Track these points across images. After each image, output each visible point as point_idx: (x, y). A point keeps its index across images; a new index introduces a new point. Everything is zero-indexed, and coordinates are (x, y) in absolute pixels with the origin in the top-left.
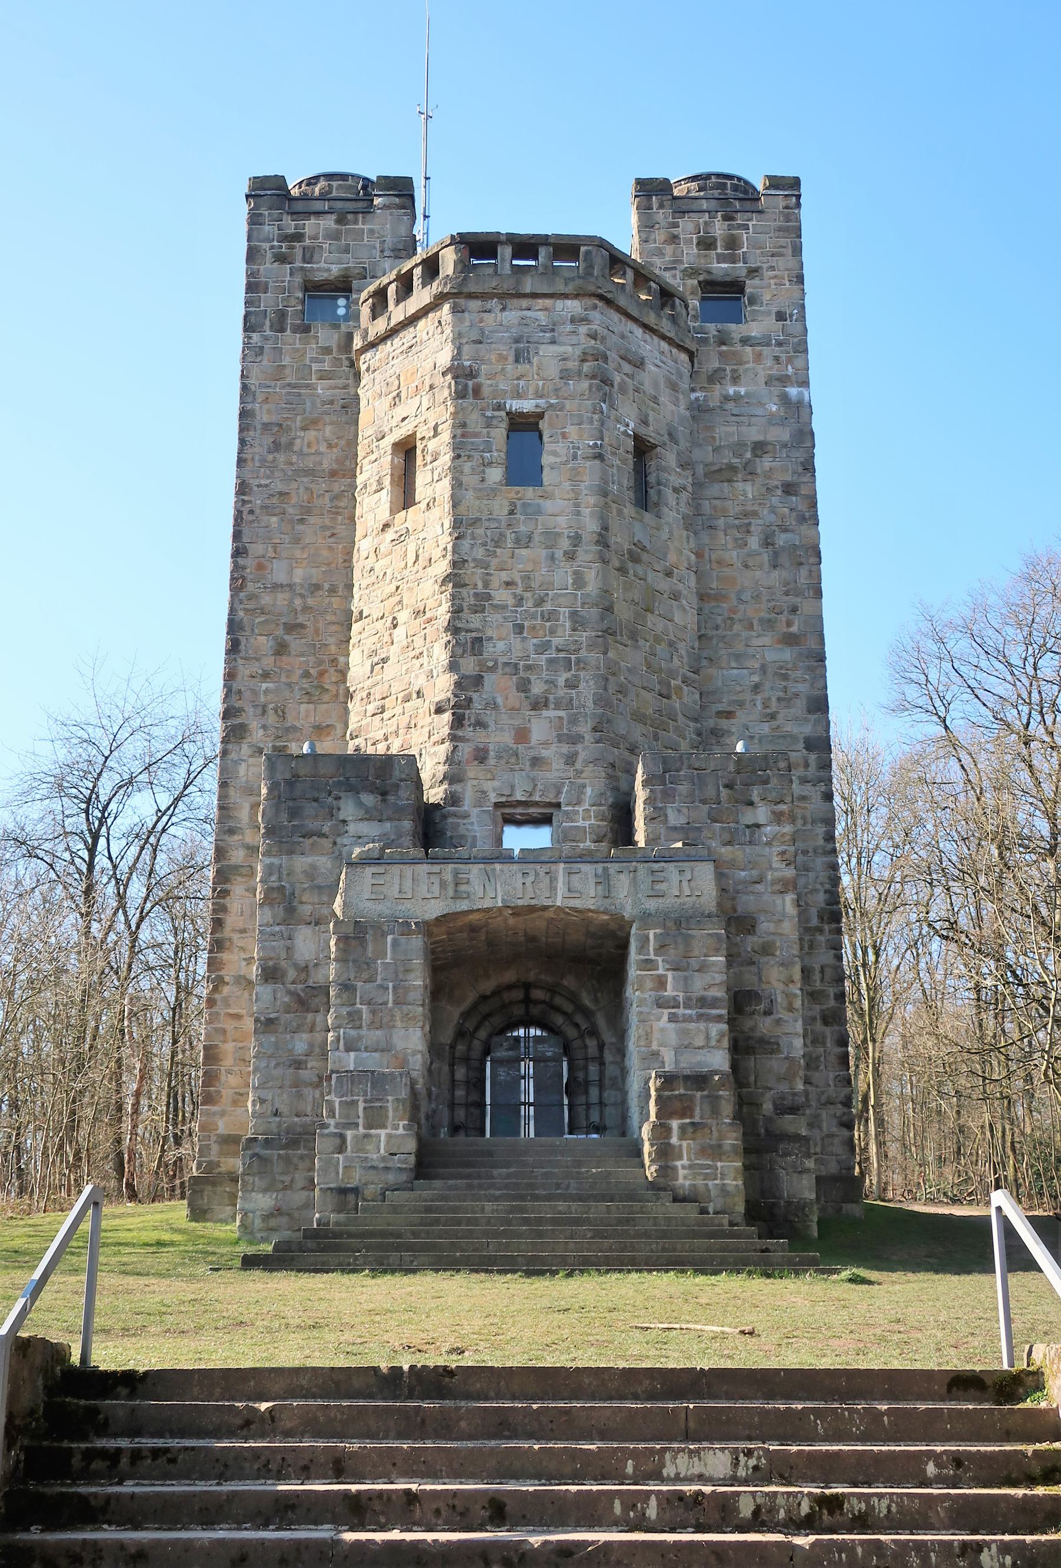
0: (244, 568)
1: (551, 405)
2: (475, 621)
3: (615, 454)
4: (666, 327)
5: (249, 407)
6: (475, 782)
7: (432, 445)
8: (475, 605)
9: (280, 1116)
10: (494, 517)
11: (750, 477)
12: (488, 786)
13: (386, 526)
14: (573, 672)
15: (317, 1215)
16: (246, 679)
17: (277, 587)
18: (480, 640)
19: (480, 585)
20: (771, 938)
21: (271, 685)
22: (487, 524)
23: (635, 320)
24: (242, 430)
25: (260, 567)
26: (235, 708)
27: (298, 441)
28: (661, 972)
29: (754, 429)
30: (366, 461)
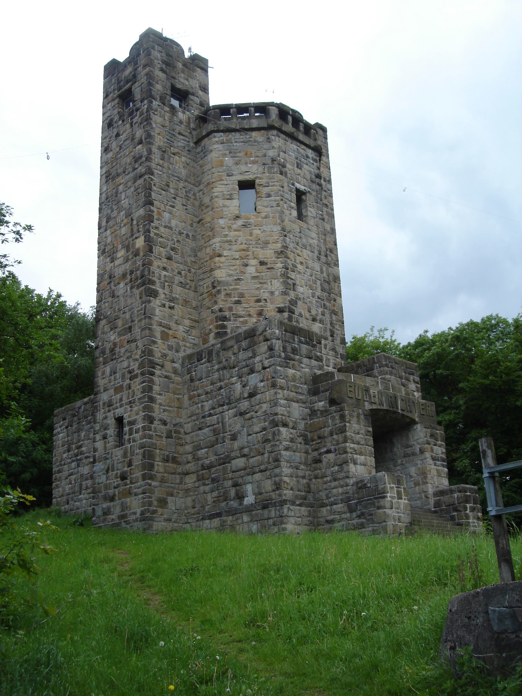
19: (293, 260)
25: (159, 214)
27: (172, 159)
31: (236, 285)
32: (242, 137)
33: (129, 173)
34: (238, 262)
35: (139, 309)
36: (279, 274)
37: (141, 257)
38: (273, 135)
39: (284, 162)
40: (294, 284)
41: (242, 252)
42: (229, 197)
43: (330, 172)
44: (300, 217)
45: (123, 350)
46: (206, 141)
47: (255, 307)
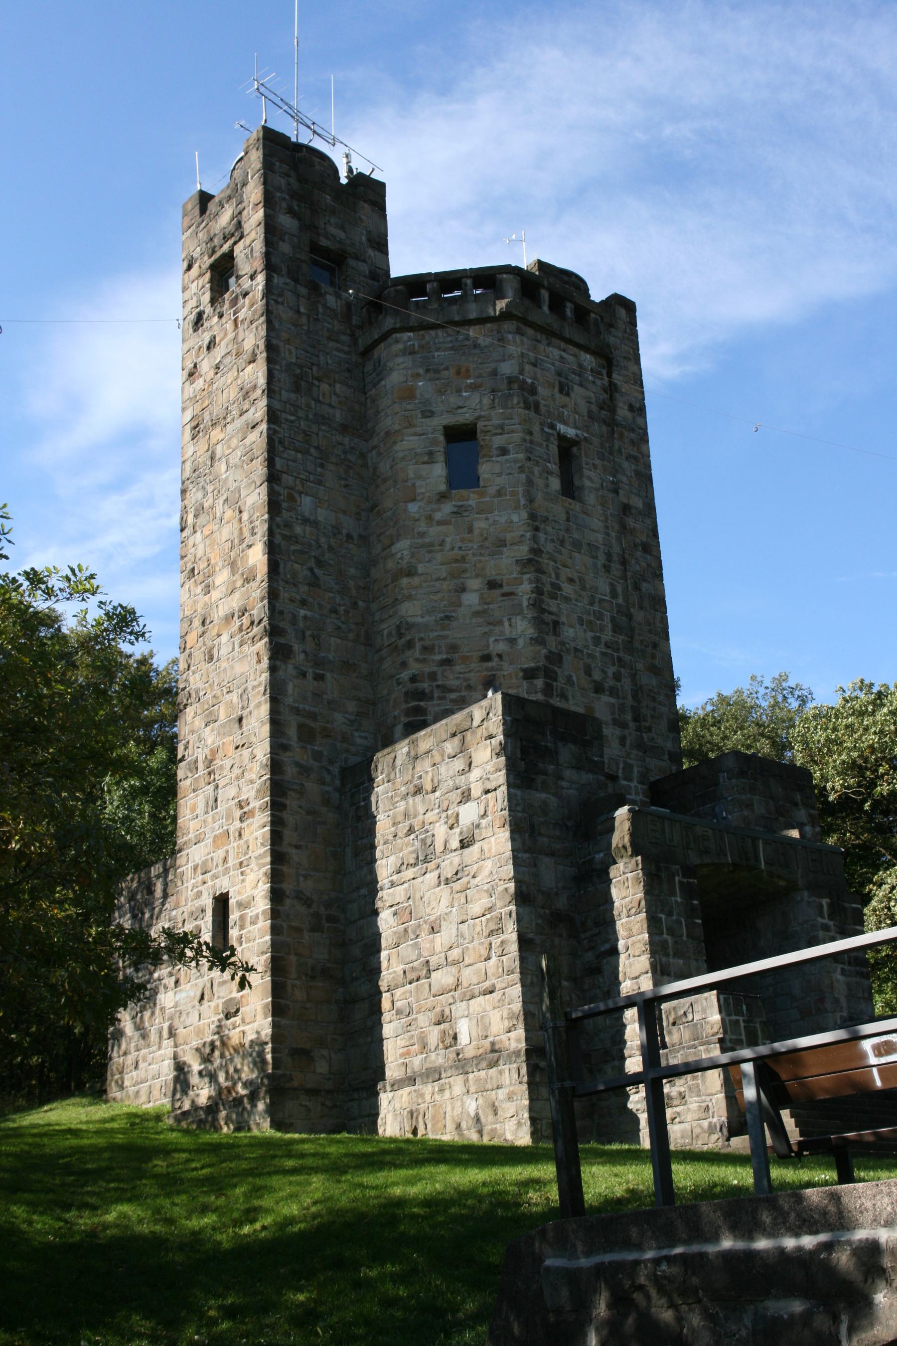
0: (279, 494)
1: (585, 438)
5: (274, 342)
13: (443, 497)
17: (306, 521)
19: (553, 575)
21: (309, 614)
25: (291, 498)
27: (315, 389)
31: (443, 629)
32: (449, 339)
33: (233, 420)
34: (445, 585)
35: (255, 683)
36: (525, 604)
37: (257, 584)
38: (510, 333)
39: (533, 383)
40: (556, 624)
41: (454, 565)
42: (426, 458)
43: (643, 393)
44: (569, 489)
45: (228, 763)
46: (381, 351)
47: (478, 671)
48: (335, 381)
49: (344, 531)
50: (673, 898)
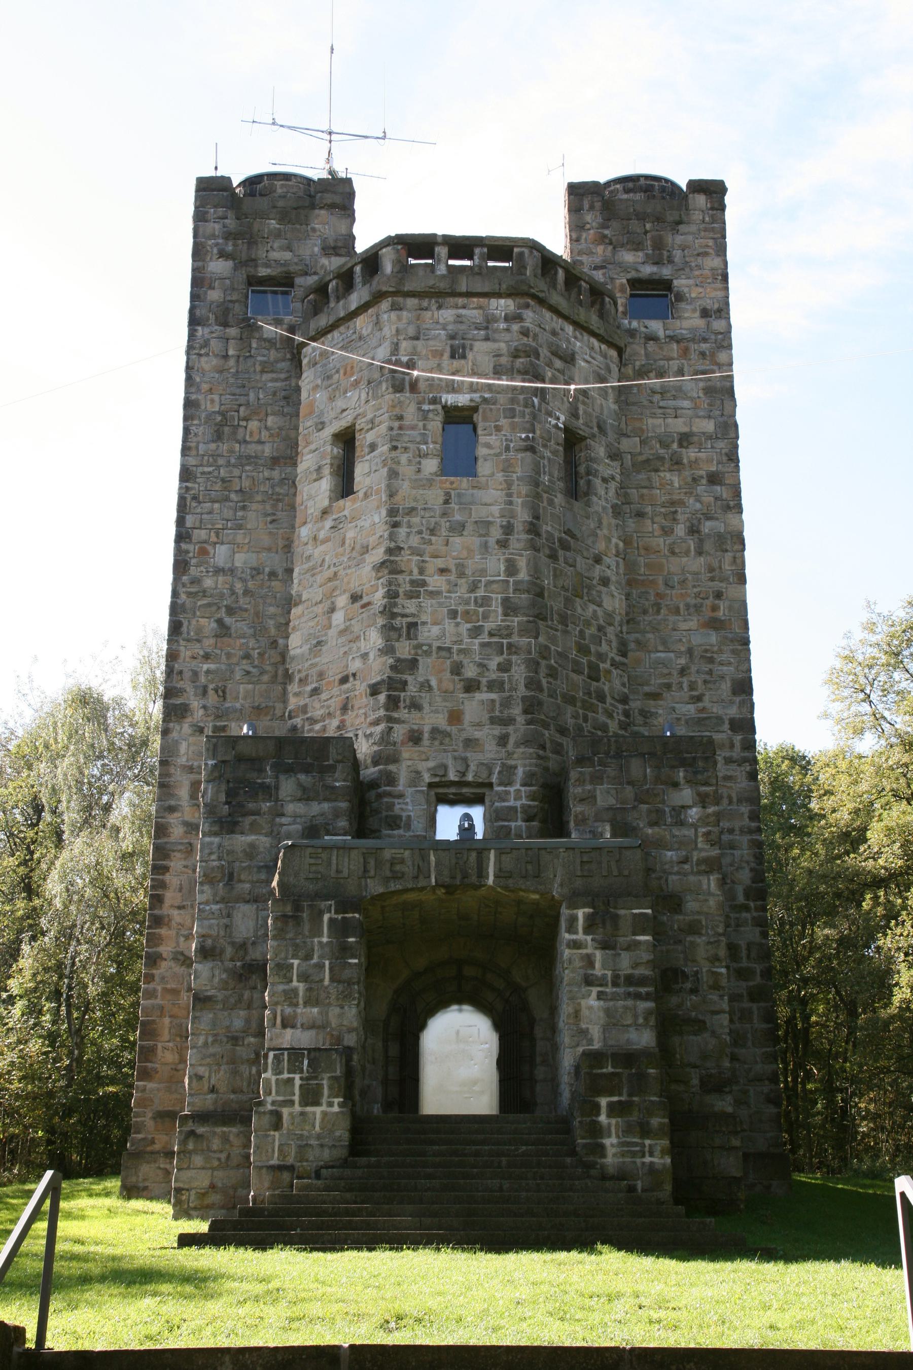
0: (187, 552)
1: (485, 400)
2: (410, 606)
3: (545, 446)
4: (594, 321)
5: (193, 397)
6: (409, 763)
7: (370, 437)
8: (411, 591)
9: (217, 1092)
10: (429, 506)
11: (676, 467)
12: (423, 766)
14: (505, 656)
15: (252, 1193)
16: (187, 659)
17: (218, 571)
18: (415, 625)
19: (416, 571)
20: (696, 917)
22: (422, 513)
23: (566, 318)
24: (186, 418)
25: (203, 552)
26: (176, 688)
28: (589, 951)
29: (680, 420)
30: (306, 451)
31: (315, 657)
48: (267, 415)
49: (267, 570)
50: (316, 940)
